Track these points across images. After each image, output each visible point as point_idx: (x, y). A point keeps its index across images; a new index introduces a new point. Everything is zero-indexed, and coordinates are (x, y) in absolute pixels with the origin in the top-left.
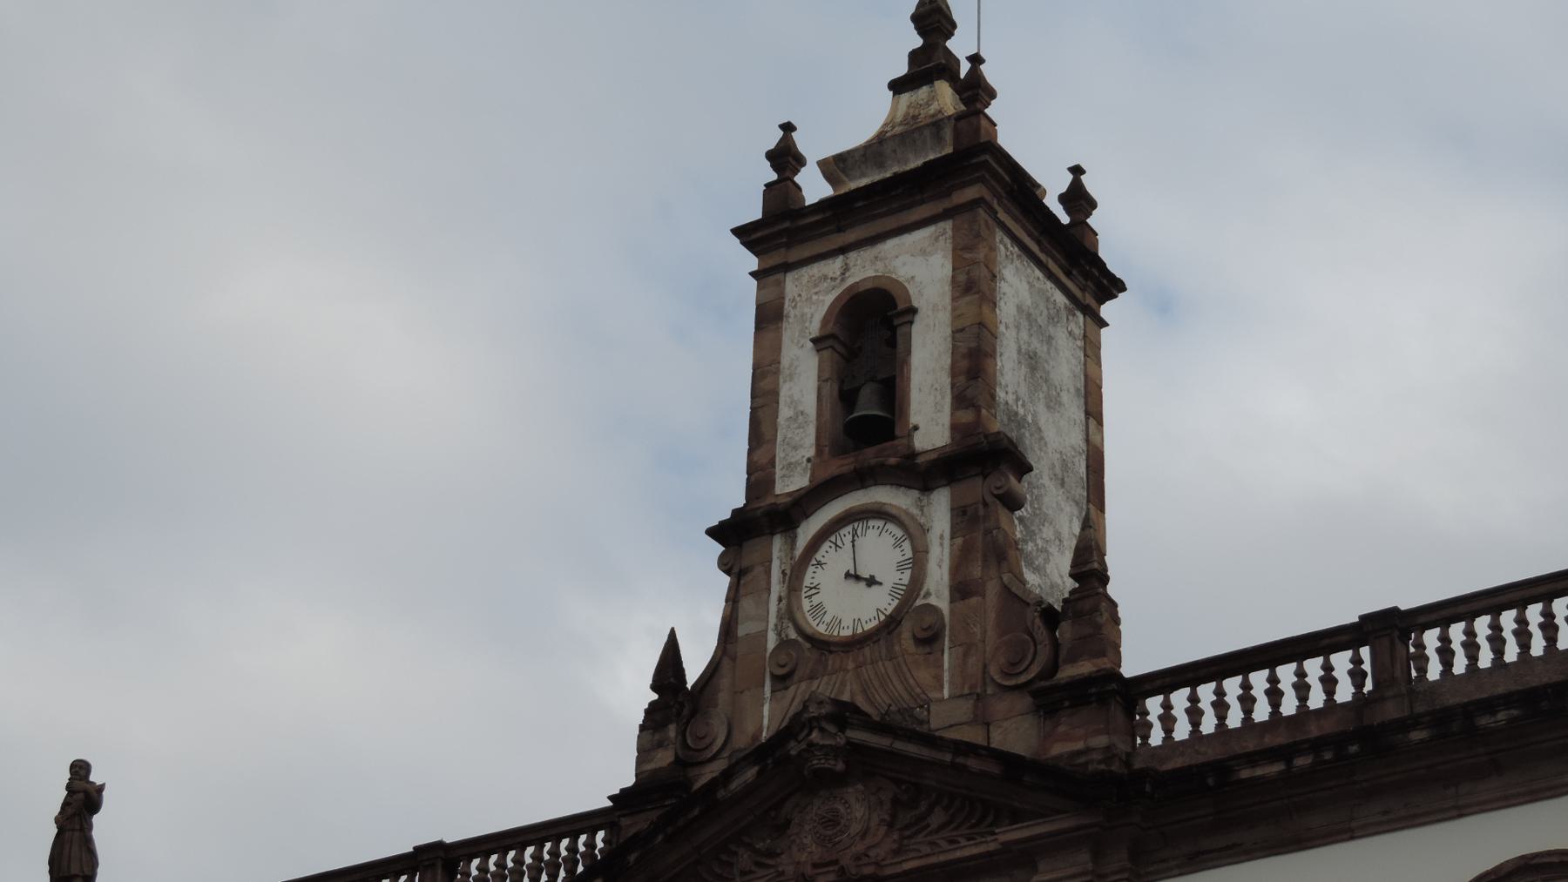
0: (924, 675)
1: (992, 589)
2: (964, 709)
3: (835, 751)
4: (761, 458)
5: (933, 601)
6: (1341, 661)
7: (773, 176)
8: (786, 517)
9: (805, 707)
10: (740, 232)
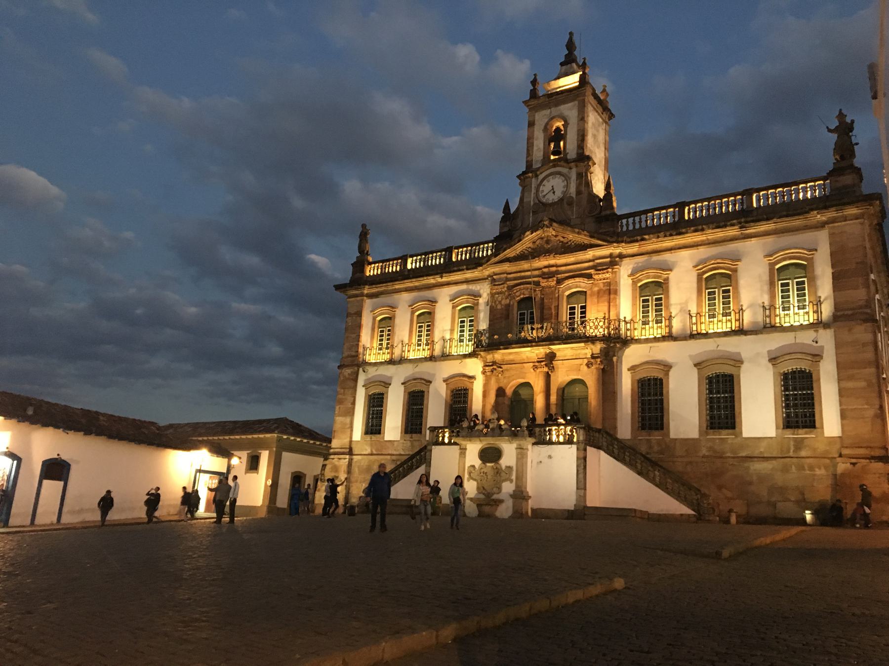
0: (569, 213)
5: (571, 195)
7: (532, 88)
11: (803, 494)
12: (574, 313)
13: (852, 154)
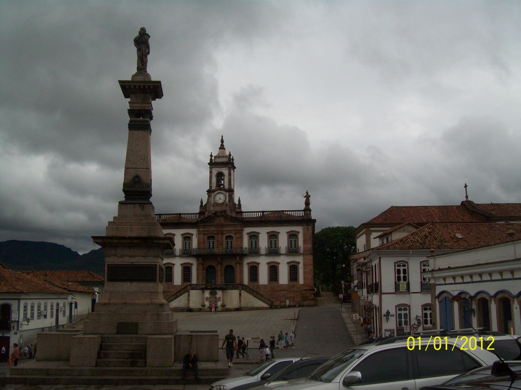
1: (232, 202)
2: (229, 212)
3: (221, 215)
4: (210, 185)
6: (259, 213)
8: (214, 191)
9: (218, 211)
10: (208, 163)
11: (294, 299)
12: (228, 243)
13: (309, 204)
